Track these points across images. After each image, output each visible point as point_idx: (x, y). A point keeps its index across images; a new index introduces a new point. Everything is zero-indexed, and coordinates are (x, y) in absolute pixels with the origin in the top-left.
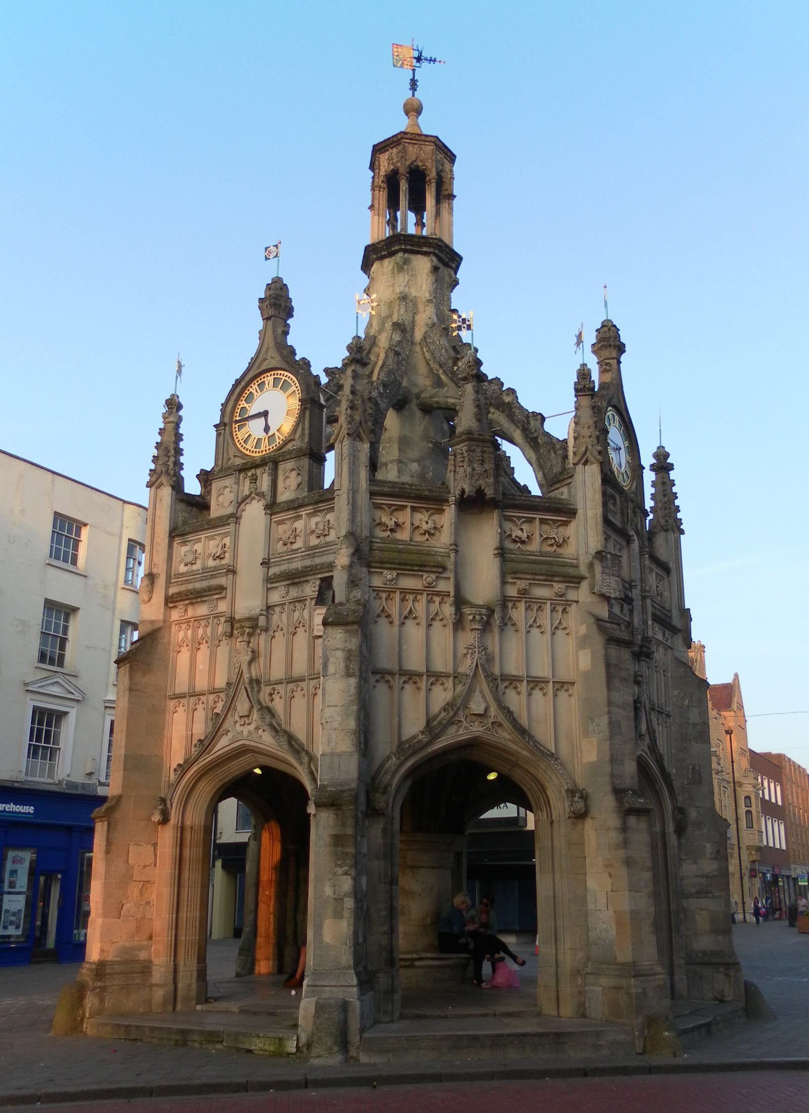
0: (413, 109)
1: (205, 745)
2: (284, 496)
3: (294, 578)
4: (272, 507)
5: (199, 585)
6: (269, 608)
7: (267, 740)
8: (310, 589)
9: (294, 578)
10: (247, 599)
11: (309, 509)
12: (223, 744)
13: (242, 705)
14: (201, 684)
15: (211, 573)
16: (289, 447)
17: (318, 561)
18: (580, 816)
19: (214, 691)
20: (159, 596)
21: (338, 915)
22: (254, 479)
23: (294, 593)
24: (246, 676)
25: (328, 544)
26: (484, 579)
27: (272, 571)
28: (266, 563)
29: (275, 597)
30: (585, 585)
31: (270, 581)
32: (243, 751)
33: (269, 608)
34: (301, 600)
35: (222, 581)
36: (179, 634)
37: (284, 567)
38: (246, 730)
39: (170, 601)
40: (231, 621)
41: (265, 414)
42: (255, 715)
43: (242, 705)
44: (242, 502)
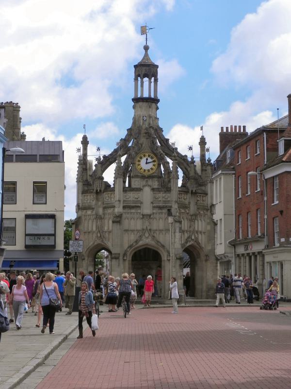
0: (146, 48)
1: (137, 242)
2: (156, 187)
3: (160, 208)
4: (153, 189)
5: (132, 205)
6: (153, 213)
7: (153, 243)
8: (165, 211)
9: (160, 208)
10: (147, 209)
11: (163, 192)
12: (141, 243)
13: (147, 235)
14: (132, 228)
15: (134, 202)
16: (155, 174)
17: (167, 205)
18: (206, 260)
19: (137, 230)
20: (121, 207)
21: (181, 279)
22: (147, 181)
23: (160, 211)
24: (149, 228)
25: (169, 201)
26: (193, 209)
27: (154, 205)
28: (152, 203)
29: (154, 211)
30: (209, 211)
31: (154, 207)
32: (147, 244)
33: (153, 213)
34: (162, 213)
35: (139, 205)
36: (124, 216)
37: (158, 205)
38: (147, 240)
39: (124, 207)
40: (143, 215)
41: (147, 163)
42: (150, 237)
43: (147, 235)
44: (144, 186)
